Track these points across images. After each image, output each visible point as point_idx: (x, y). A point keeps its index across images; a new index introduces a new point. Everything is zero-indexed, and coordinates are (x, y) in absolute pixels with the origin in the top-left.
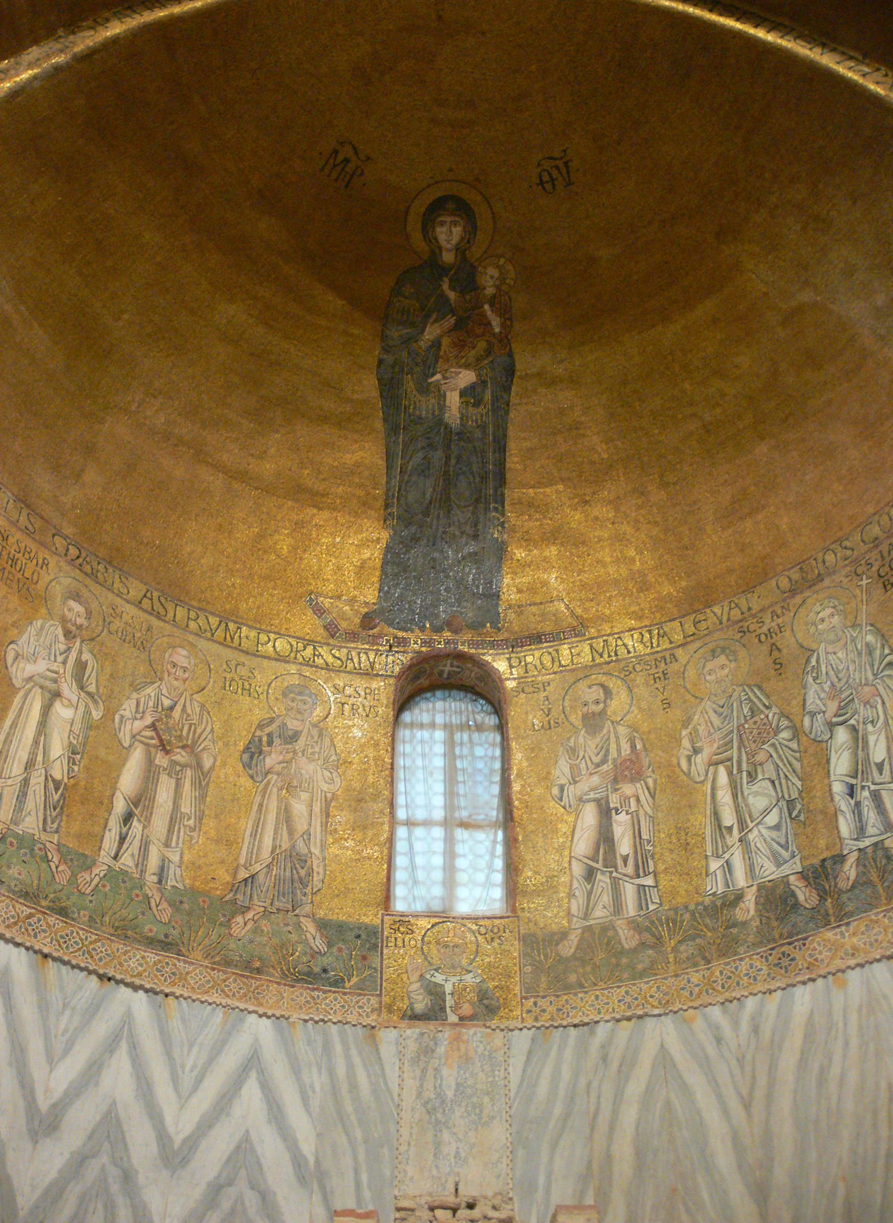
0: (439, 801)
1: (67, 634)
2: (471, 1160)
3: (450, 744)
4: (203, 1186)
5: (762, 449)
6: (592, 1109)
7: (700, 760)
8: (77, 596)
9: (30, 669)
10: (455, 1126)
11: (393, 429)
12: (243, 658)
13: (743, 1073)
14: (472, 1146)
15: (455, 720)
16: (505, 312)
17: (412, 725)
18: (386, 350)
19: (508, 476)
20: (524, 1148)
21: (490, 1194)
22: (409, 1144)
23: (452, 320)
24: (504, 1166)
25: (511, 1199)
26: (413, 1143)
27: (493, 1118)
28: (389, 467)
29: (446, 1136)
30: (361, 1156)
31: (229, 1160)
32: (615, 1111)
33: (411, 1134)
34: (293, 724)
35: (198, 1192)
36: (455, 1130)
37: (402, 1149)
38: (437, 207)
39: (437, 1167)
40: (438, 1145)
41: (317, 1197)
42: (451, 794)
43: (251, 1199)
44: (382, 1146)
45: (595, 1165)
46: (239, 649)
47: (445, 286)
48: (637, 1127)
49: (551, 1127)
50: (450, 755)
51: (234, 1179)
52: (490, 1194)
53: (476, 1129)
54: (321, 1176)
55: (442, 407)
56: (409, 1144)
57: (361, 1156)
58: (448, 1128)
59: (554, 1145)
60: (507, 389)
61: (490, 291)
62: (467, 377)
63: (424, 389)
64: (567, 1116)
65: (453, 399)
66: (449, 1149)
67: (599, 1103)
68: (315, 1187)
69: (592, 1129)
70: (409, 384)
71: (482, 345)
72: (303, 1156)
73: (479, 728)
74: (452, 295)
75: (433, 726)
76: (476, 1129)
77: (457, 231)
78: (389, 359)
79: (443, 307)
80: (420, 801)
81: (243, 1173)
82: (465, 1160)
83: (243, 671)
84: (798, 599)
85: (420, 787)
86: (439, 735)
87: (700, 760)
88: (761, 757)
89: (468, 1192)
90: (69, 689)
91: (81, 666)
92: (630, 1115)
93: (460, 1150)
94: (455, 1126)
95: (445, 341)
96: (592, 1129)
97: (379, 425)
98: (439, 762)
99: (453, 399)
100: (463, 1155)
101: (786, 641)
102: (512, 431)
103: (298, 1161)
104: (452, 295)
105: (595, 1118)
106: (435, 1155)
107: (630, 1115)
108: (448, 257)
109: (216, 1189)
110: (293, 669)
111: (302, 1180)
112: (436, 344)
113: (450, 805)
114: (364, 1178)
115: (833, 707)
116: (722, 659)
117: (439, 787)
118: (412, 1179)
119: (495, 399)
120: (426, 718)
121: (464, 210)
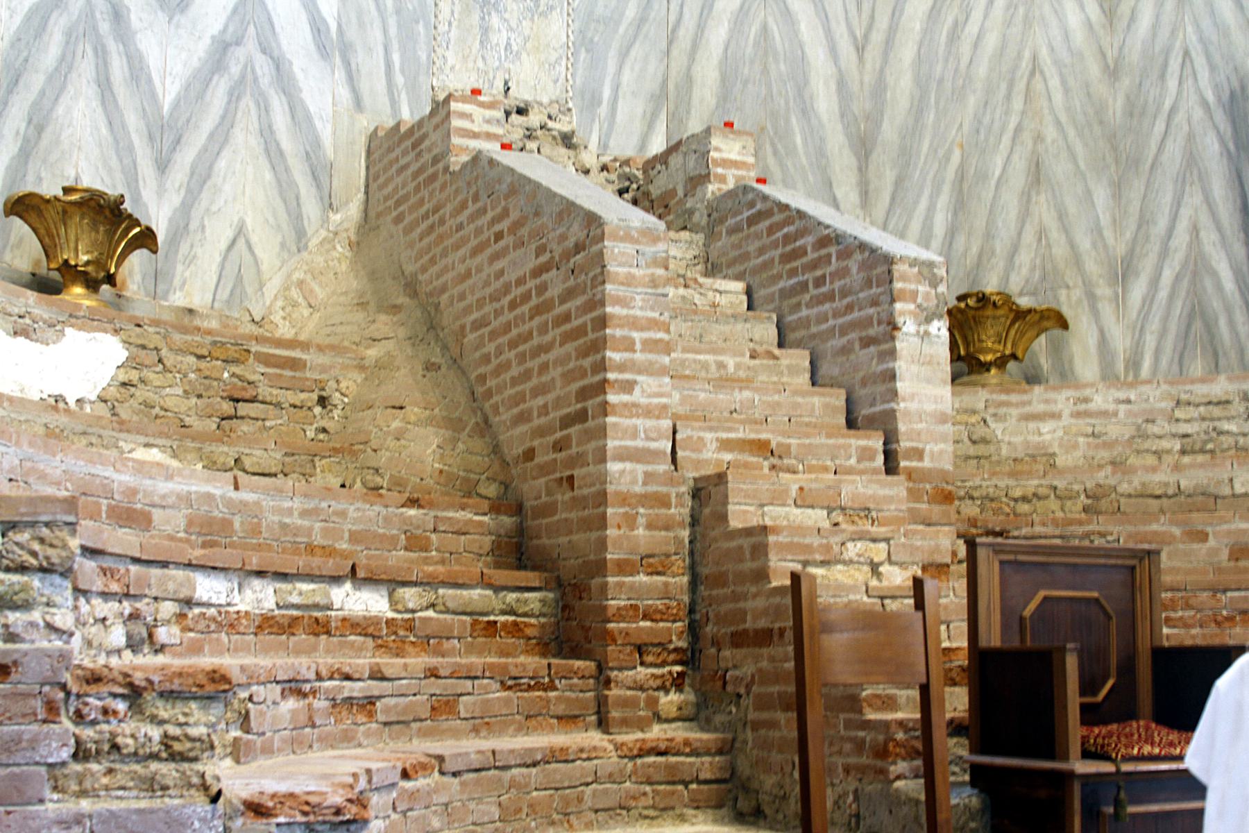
2: (524, 56)
4: (207, 41)
6: (672, 18)
10: (506, 11)
13: (860, 16)
14: (526, 40)
20: (587, 51)
21: (545, 100)
22: (450, 24)
24: (563, 69)
25: (569, 110)
26: (455, 24)
27: (552, 8)
29: (495, 21)
30: (393, 31)
31: (235, 11)
32: (701, 28)
33: (453, 12)
35: (202, 47)
36: (507, 16)
37: (443, 28)
39: (483, 58)
40: (486, 30)
41: (340, 74)
43: (263, 66)
44: (417, 22)
45: (671, 86)
48: (726, 49)
49: (622, 30)
51: (243, 37)
52: (545, 100)
53: (532, 20)
54: (346, 49)
56: (450, 24)
57: (393, 31)
58: (497, 11)
59: (624, 55)
64: (641, 21)
66: (499, 37)
67: (681, 13)
68: (338, 60)
69: (670, 43)
72: (324, 21)
76: (532, 20)
81: (251, 29)
82: (518, 54)
89: (521, 94)
92: (718, 34)
93: (512, 41)
94: (506, 11)
96: (670, 43)
100: (515, 48)
103: (317, 26)
105: (674, 31)
106: (481, 42)
107: (718, 34)
109: (223, 47)
111: (323, 50)
114: (396, 57)
118: (452, 68)
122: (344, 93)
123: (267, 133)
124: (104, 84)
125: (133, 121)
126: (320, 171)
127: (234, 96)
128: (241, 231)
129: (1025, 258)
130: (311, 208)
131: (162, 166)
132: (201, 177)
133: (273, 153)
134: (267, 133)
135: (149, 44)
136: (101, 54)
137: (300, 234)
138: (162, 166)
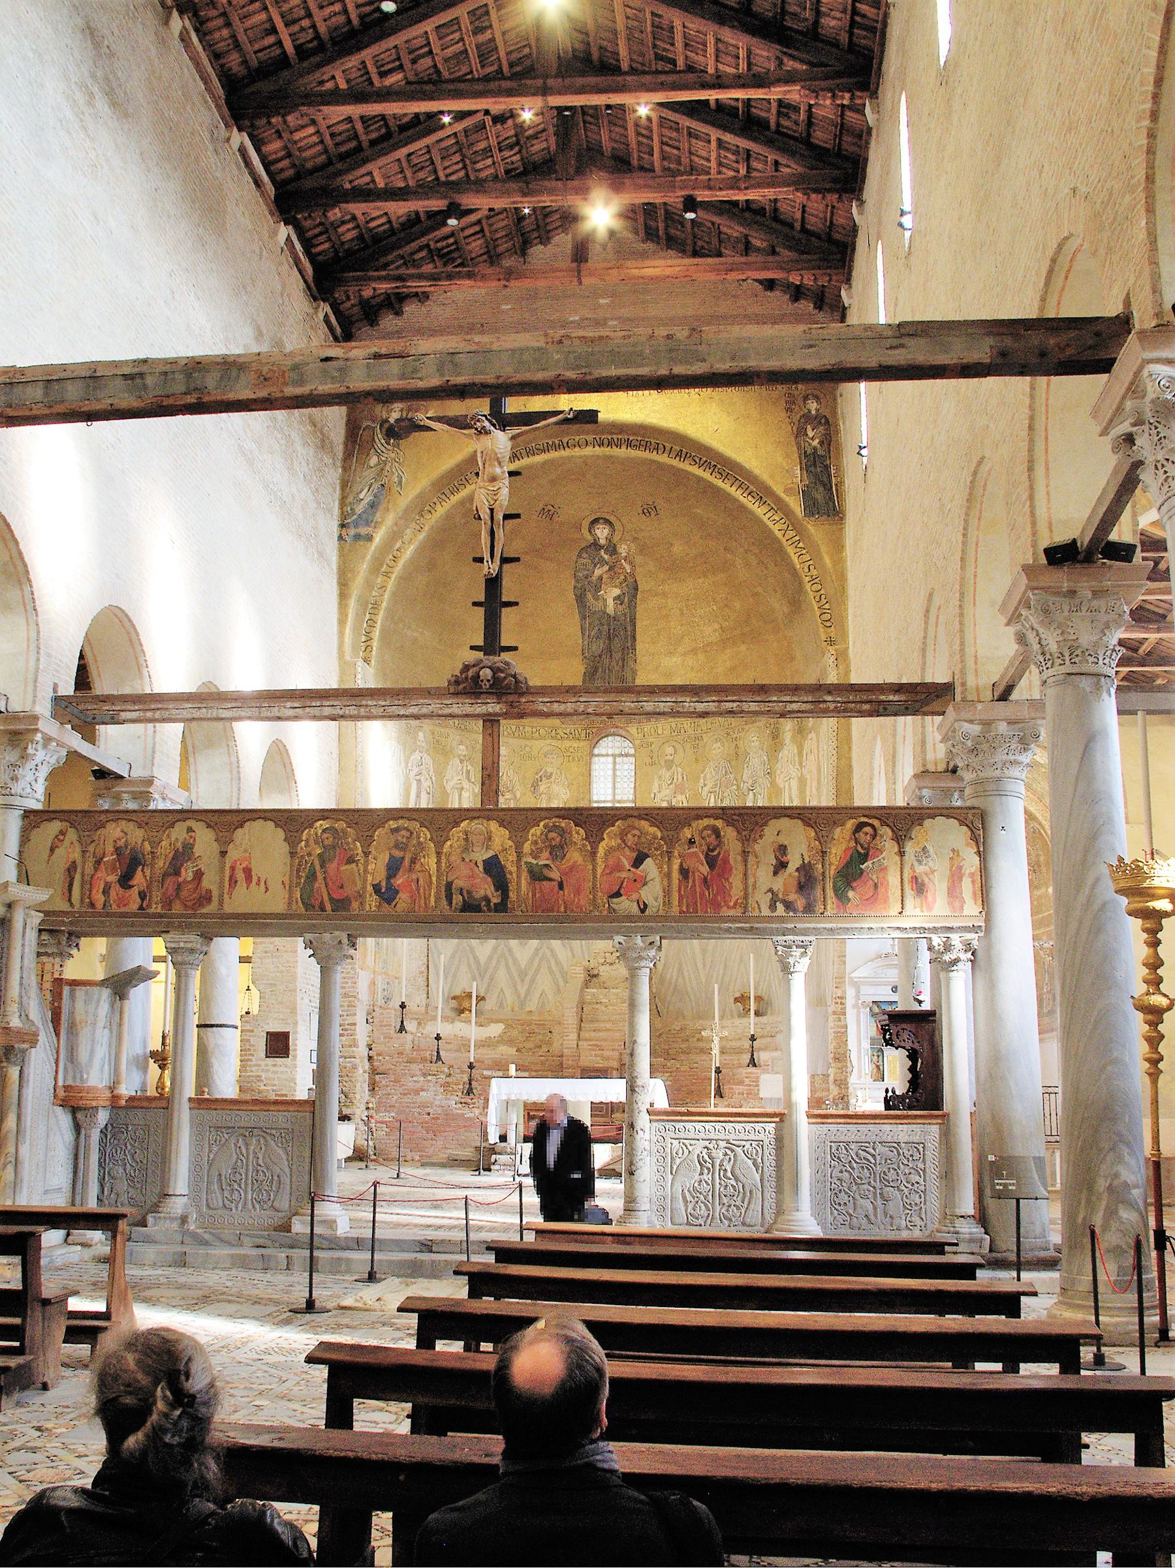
0: (610, 791)
1: (461, 761)
3: (615, 763)
5: (743, 648)
7: (706, 789)
8: (461, 743)
9: (451, 783)
11: (583, 618)
12: (527, 742)
15: (617, 752)
16: (631, 563)
17: (598, 755)
18: (577, 581)
19: (637, 637)
23: (606, 568)
28: (583, 634)
34: (549, 770)
38: (595, 521)
42: (614, 788)
43: (548, 953)
46: (525, 738)
47: (602, 552)
50: (614, 770)
55: (605, 606)
60: (635, 596)
61: (624, 554)
62: (616, 592)
63: (597, 598)
65: (610, 603)
70: (589, 596)
71: (622, 577)
73: (627, 755)
74: (606, 557)
75: (607, 755)
77: (606, 531)
78: (579, 585)
79: (602, 562)
80: (602, 792)
83: (528, 749)
84: (746, 727)
85: (602, 785)
86: (610, 759)
87: (706, 789)
88: (726, 794)
90: (466, 784)
91: (468, 772)
95: (605, 576)
97: (577, 617)
98: (610, 773)
99: (610, 603)
101: (740, 744)
102: (638, 616)
104: (606, 557)
108: (602, 542)
110: (548, 742)
112: (601, 578)
113: (614, 794)
115: (750, 782)
116: (719, 744)
117: (610, 785)
119: (630, 601)
120: (604, 752)
121: (608, 522)
122: (570, 954)
123: (550, 968)
124: (507, 966)
125: (515, 974)
126: (564, 975)
127: (541, 960)
128: (543, 991)
129: (738, 982)
130: (561, 983)
131: (522, 981)
132: (533, 981)
133: (551, 972)
134: (550, 968)
135: (518, 955)
136: (506, 960)
137: (559, 990)
138: (522, 981)
